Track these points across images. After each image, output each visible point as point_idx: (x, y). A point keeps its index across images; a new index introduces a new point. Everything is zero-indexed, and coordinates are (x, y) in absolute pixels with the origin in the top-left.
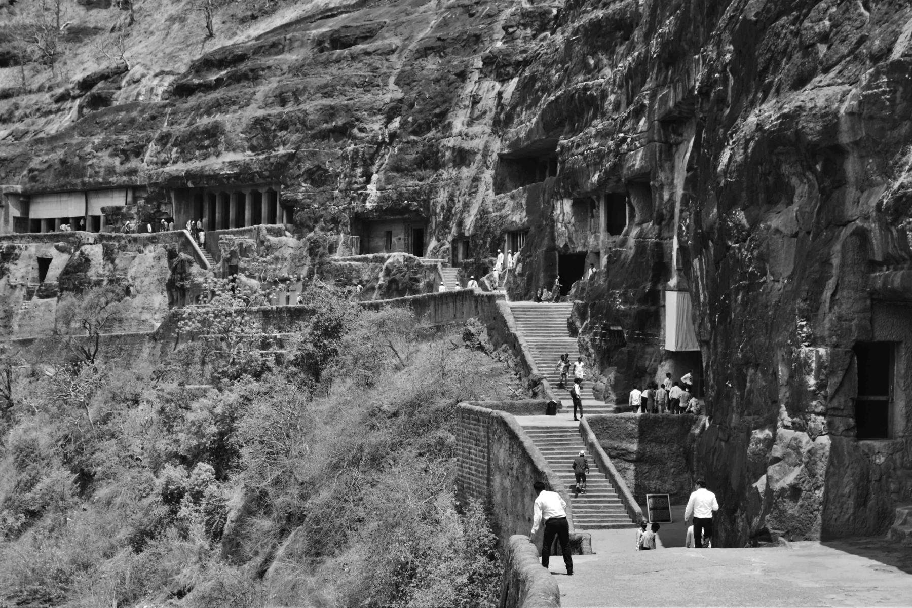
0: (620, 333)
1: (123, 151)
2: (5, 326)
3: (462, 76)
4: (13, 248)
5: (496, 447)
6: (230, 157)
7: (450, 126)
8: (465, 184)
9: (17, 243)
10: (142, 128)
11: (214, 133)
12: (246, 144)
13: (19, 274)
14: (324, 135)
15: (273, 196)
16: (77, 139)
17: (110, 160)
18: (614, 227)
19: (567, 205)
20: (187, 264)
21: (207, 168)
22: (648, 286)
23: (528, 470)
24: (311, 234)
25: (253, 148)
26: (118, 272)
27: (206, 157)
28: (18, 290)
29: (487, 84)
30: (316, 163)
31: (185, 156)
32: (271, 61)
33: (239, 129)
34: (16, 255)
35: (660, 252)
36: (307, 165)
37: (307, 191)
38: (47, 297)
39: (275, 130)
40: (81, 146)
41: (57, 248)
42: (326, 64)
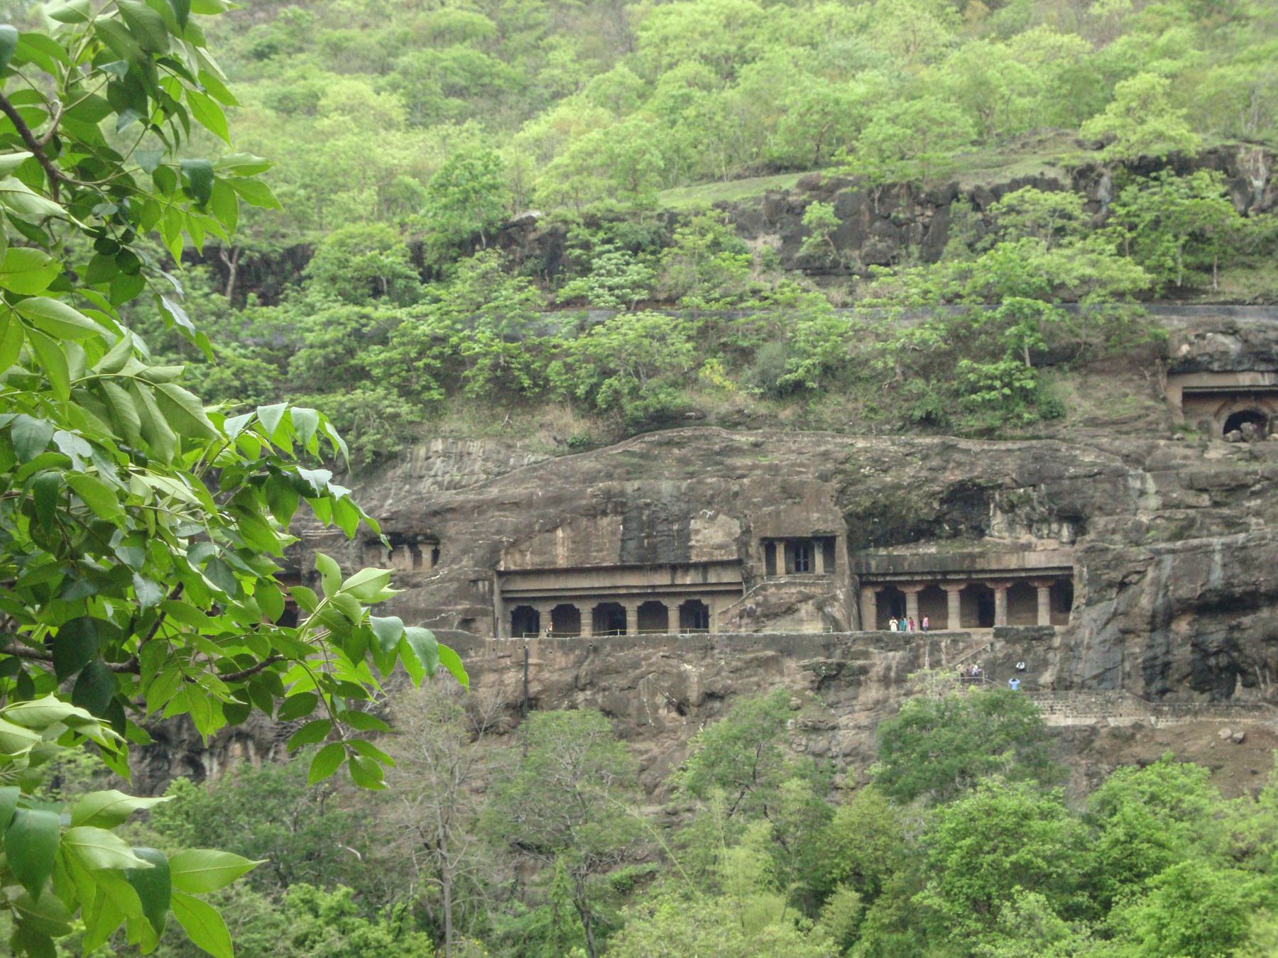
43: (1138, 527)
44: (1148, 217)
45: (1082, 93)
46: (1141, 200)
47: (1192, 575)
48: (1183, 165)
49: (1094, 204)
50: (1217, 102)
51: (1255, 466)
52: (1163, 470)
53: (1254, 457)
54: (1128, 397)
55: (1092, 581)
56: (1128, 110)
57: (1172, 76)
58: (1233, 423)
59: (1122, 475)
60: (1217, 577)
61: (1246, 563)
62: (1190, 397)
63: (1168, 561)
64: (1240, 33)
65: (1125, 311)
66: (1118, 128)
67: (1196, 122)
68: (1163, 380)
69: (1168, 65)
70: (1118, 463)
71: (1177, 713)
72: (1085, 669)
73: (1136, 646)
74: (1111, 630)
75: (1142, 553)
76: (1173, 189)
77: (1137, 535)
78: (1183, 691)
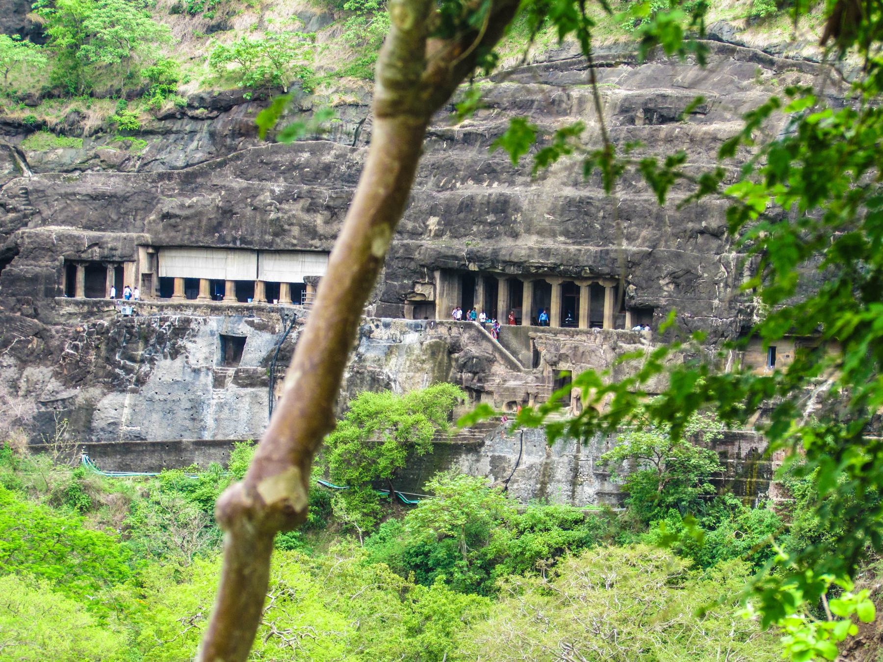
1: (328, 207)
2: (194, 419)
4: (188, 321)
9: (188, 313)
11: (502, 207)
12: (557, 228)
13: (201, 356)
15: (597, 294)
17: (306, 217)
20: (485, 363)
21: (503, 252)
24: (685, 346)
25: (566, 233)
26: (368, 364)
28: (202, 375)
30: (683, 266)
33: (542, 208)
34: (193, 330)
36: (670, 267)
37: (670, 296)
38: (252, 385)
39: (604, 217)
41: (251, 324)
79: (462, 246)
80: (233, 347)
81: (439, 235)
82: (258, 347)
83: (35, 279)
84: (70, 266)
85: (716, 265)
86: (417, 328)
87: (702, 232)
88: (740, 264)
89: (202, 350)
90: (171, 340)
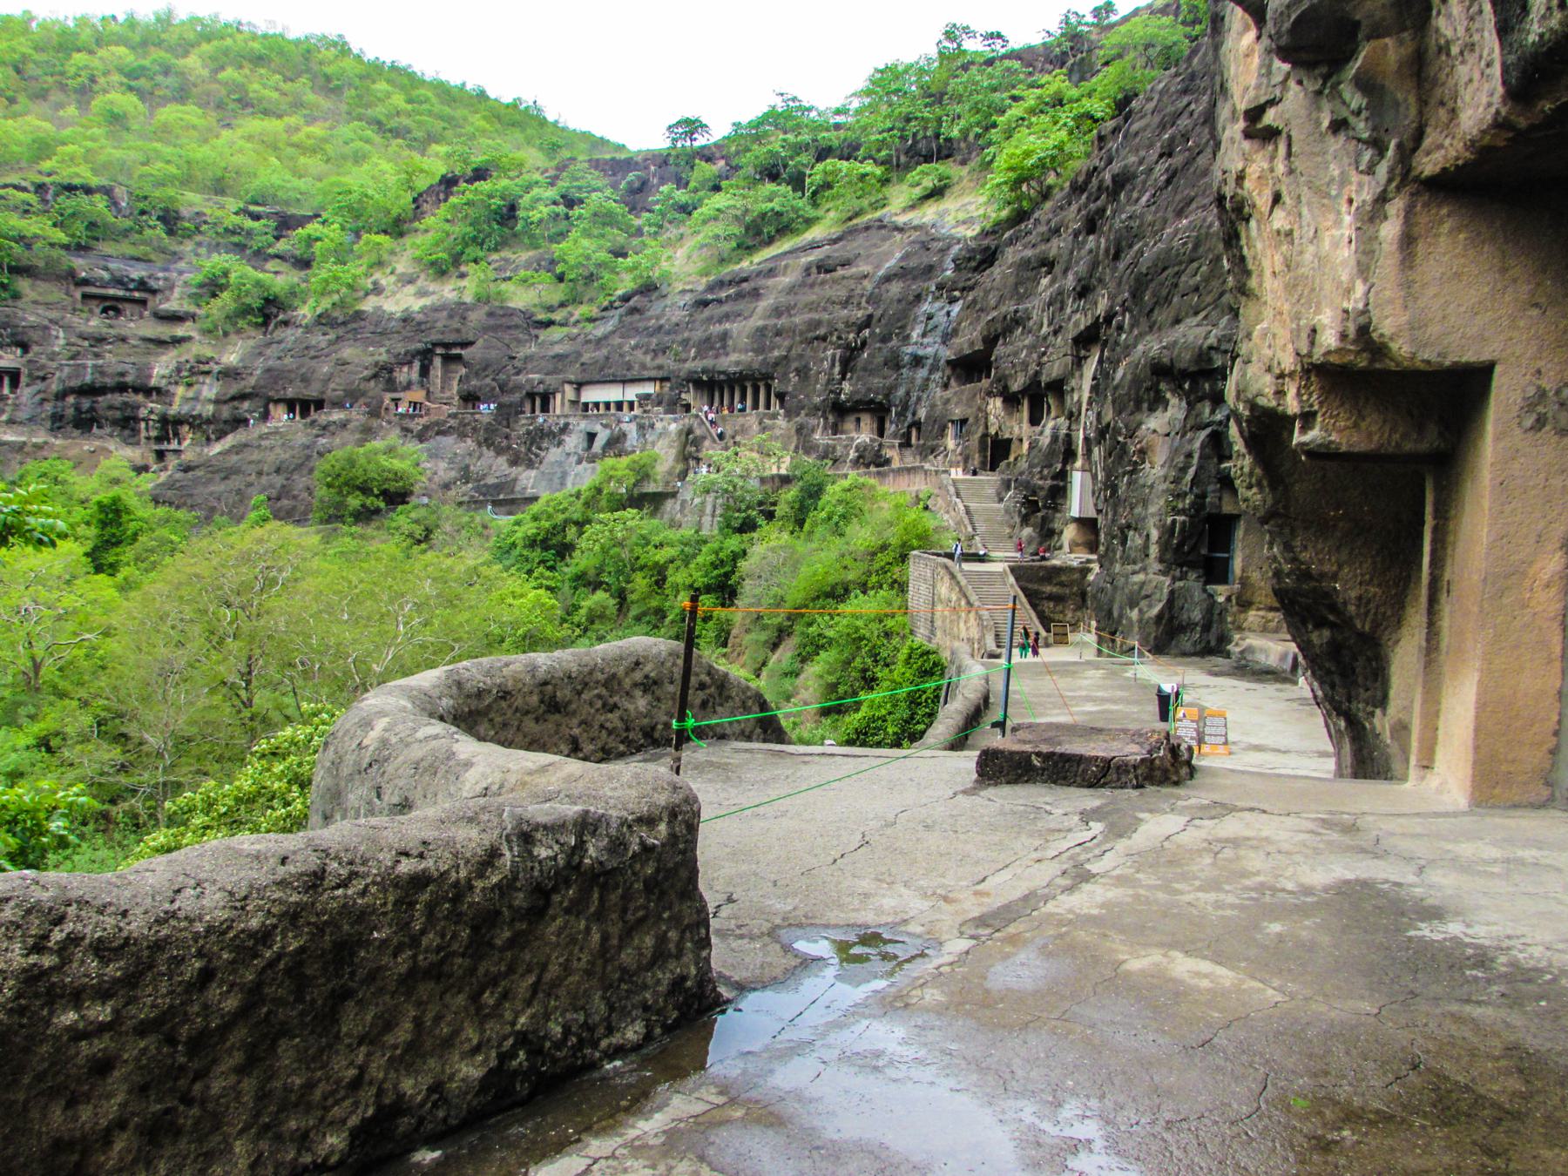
0: (1036, 502)
3: (918, 298)
5: (939, 585)
6: (734, 357)
7: (908, 337)
8: (919, 382)
9: (571, 420)
10: (668, 333)
11: (725, 336)
14: (810, 342)
15: (768, 388)
16: (617, 340)
18: (1035, 420)
19: (998, 402)
22: (1059, 466)
23: (963, 603)
27: (717, 357)
29: (937, 305)
31: (700, 355)
32: (770, 282)
35: (1069, 439)
36: (794, 365)
40: (620, 346)
42: (812, 286)
43: (54, 353)
44: (70, 211)
45: (43, 149)
46: (68, 203)
47: (77, 376)
48: (88, 191)
49: (44, 201)
50: (106, 166)
51: (112, 331)
52: (67, 328)
53: (111, 326)
54: (55, 293)
55: (30, 375)
56: (63, 161)
57: (88, 151)
58: (105, 310)
59: (46, 328)
60: (88, 379)
61: (102, 373)
62: (85, 296)
63: (66, 370)
64: (124, 134)
65: (57, 253)
66: (59, 168)
67: (95, 172)
68: (72, 287)
69: (89, 144)
70: (46, 322)
71: (65, 438)
72: (23, 415)
73: (48, 407)
74: (38, 397)
75: (54, 365)
76: (82, 201)
77: (53, 356)
78: (69, 428)
79: (694, 366)
80: (591, 437)
81: (694, 358)
82: (603, 436)
83: (510, 405)
84: (531, 396)
85: (822, 360)
86: (675, 420)
87: (817, 338)
88: (834, 356)
89: (573, 442)
90: (557, 435)
